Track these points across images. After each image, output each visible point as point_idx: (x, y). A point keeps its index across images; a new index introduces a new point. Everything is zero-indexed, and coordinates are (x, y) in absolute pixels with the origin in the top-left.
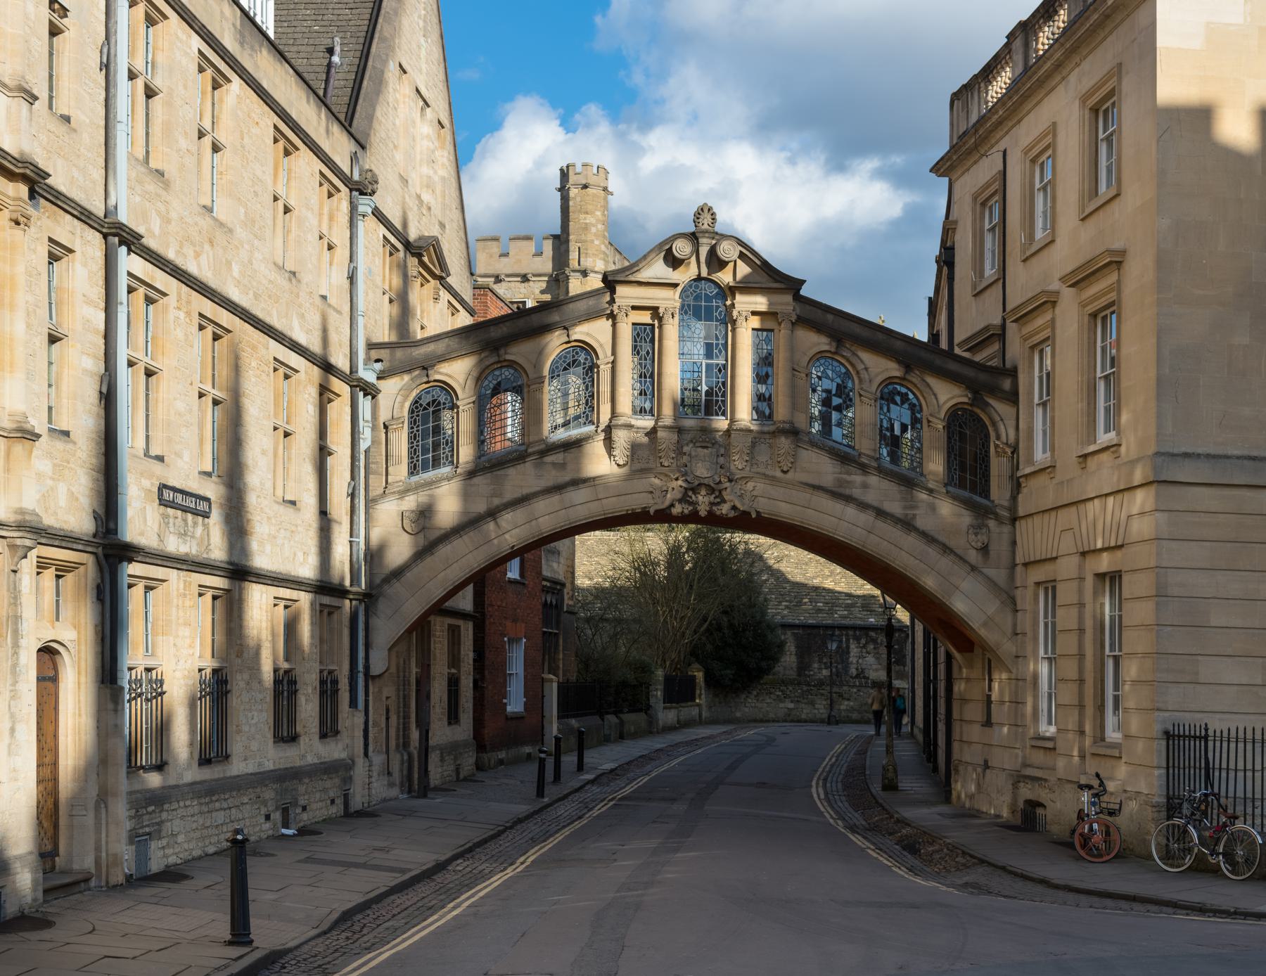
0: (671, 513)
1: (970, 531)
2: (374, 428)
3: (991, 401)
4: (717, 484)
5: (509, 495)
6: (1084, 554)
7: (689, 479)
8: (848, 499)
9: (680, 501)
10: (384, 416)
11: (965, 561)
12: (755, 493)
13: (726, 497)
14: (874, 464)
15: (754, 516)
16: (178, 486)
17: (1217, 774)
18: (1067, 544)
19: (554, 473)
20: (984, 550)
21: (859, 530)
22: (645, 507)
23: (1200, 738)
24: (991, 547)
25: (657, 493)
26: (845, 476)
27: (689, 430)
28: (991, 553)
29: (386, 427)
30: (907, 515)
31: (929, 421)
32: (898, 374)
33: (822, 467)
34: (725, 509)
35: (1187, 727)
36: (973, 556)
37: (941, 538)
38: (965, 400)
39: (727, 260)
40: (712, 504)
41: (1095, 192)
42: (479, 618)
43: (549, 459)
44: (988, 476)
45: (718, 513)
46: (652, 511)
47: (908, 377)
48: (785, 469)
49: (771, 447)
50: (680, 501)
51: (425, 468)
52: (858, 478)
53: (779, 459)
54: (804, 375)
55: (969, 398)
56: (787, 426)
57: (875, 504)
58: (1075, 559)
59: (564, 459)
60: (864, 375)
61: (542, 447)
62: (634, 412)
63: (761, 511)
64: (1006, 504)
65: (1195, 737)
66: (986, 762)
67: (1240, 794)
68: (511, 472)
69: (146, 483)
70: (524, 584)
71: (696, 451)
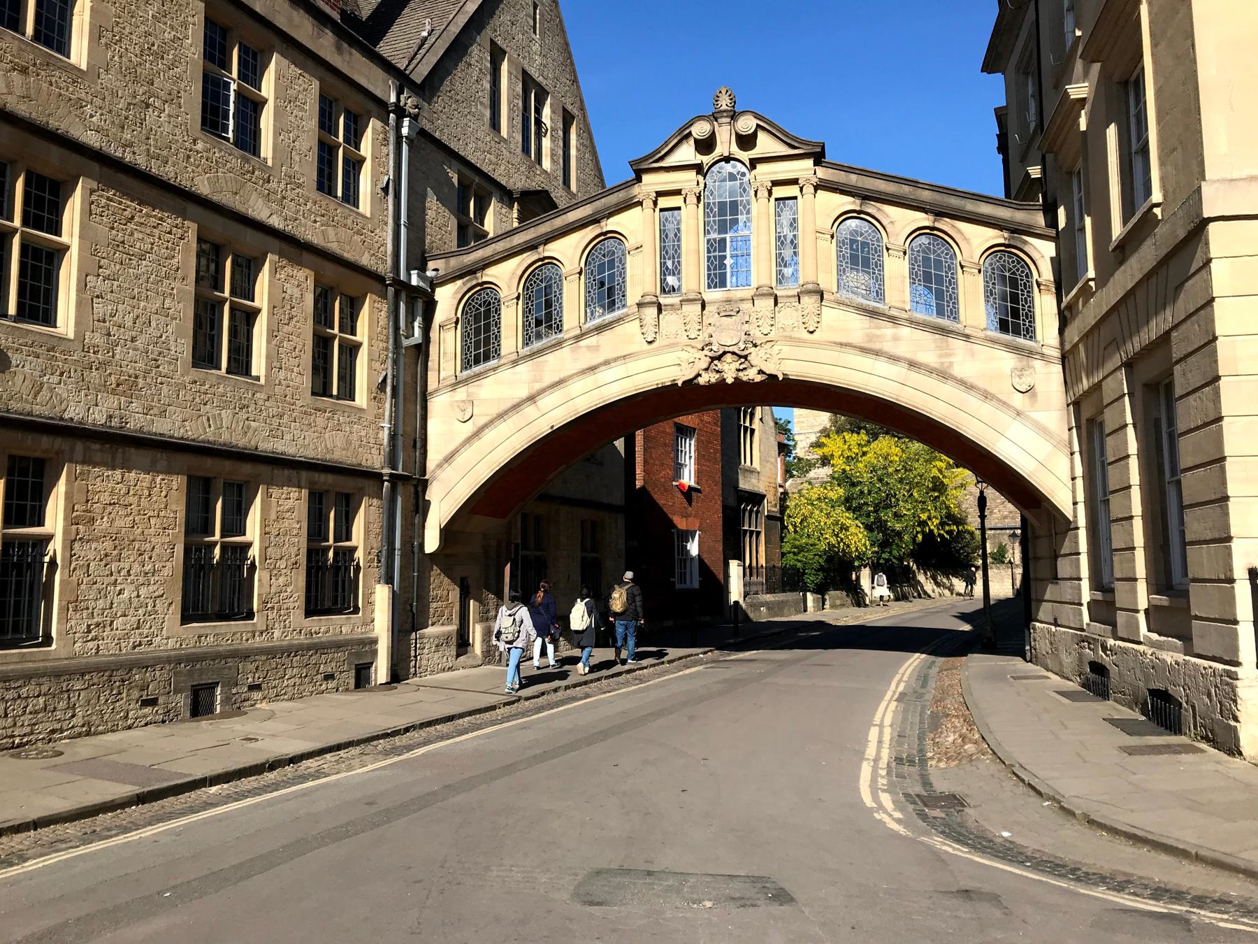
0: (698, 384)
1: (1013, 374)
4: (743, 350)
5: (548, 380)
7: (715, 348)
8: (877, 353)
9: (706, 369)
12: (779, 356)
13: (753, 363)
15: (781, 379)
22: (674, 380)
24: (1038, 389)
25: (685, 365)
26: (875, 331)
28: (1040, 396)
30: (942, 363)
31: (962, 267)
32: (927, 224)
34: (751, 375)
37: (980, 384)
39: (744, 134)
40: (738, 370)
43: (583, 343)
44: (1033, 317)
45: (745, 379)
46: (680, 385)
47: (937, 225)
48: (811, 330)
51: (477, 362)
52: (887, 330)
53: (804, 321)
54: (829, 237)
55: (1005, 239)
56: (810, 287)
57: (909, 356)
59: (598, 342)
61: (578, 332)
62: (663, 291)
63: (788, 373)
66: (1055, 619)
71: (720, 321)
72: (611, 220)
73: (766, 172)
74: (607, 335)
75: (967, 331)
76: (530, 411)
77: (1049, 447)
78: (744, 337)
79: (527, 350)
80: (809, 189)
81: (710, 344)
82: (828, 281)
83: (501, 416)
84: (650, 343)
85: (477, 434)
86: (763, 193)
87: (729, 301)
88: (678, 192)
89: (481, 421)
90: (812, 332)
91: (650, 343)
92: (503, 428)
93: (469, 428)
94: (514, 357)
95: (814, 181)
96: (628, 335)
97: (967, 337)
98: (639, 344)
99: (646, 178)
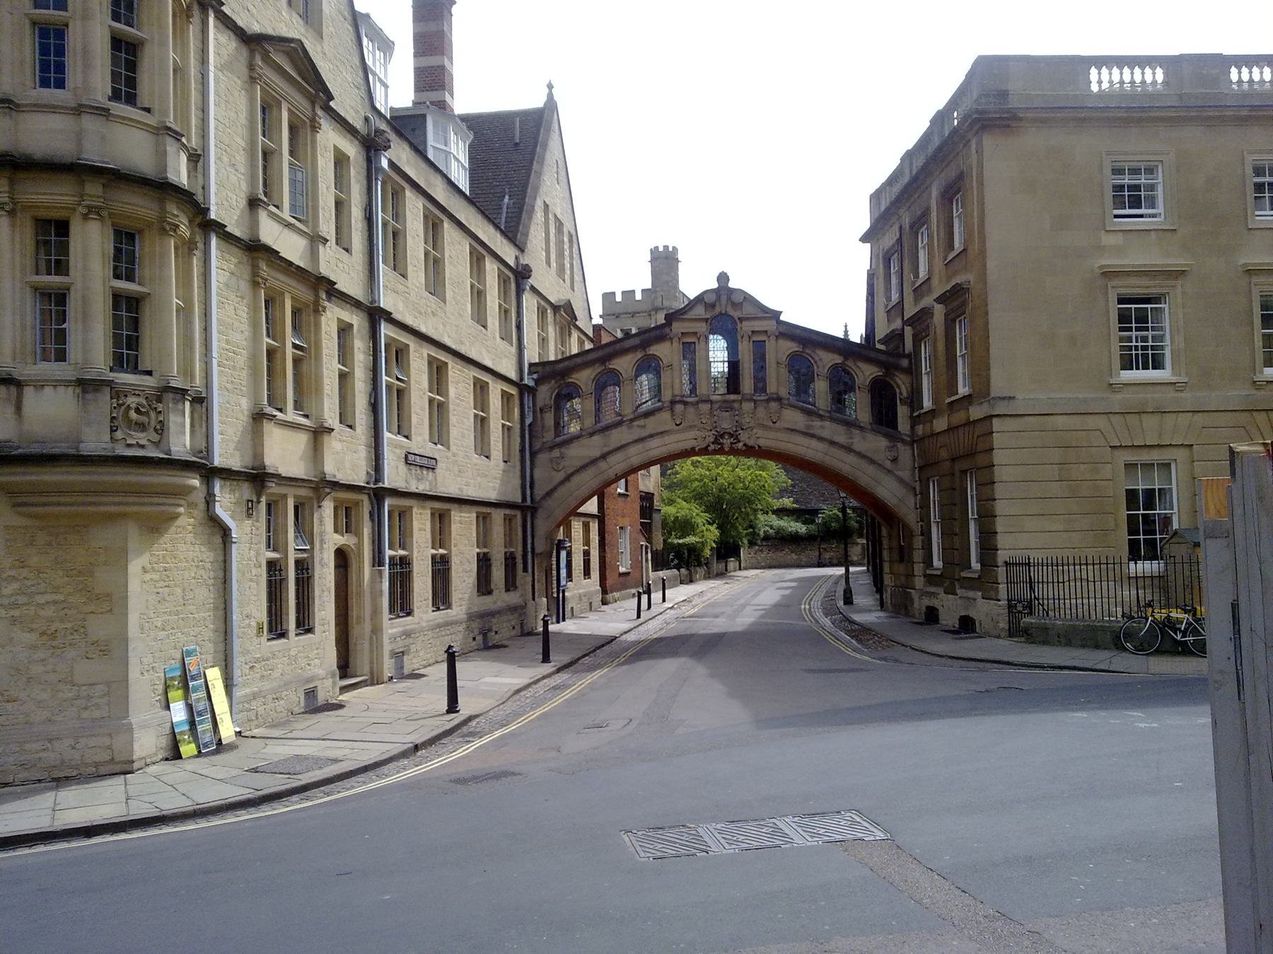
6: (953, 460)
8: (813, 436)
10: (539, 404)
11: (884, 468)
13: (742, 439)
14: (828, 415)
16: (417, 453)
17: (1036, 584)
18: (944, 454)
20: (895, 460)
21: (819, 454)
23: (1026, 564)
25: (699, 439)
27: (717, 402)
29: (541, 410)
31: (859, 388)
32: (840, 362)
34: (740, 445)
36: (888, 464)
37: (869, 455)
38: (881, 374)
40: (731, 443)
41: (951, 246)
42: (601, 517)
43: (636, 423)
46: (697, 449)
50: (713, 443)
52: (817, 423)
56: (775, 396)
57: (829, 437)
58: (948, 463)
60: (819, 363)
61: (632, 416)
64: (908, 433)
65: (1022, 564)
68: (613, 431)
69: (398, 451)
70: (628, 495)
72: (652, 348)
74: (652, 418)
75: (862, 425)
76: (603, 465)
78: (735, 423)
80: (773, 338)
81: (716, 427)
82: (783, 392)
83: (584, 467)
84: (677, 425)
86: (746, 338)
87: (725, 401)
88: (695, 333)
89: (571, 470)
91: (677, 425)
93: (560, 476)
94: (591, 431)
97: (861, 428)
98: (670, 426)
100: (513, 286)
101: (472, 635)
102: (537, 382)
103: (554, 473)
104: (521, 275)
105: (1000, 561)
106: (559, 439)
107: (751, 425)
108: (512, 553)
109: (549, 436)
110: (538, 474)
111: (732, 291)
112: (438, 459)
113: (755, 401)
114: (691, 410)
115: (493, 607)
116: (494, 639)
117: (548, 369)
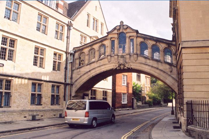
2: (74, 60)
3: (172, 46)
8: (147, 65)
9: (118, 67)
15: (131, 68)
19: (99, 64)
20: (171, 72)
24: (173, 71)
29: (76, 59)
33: (142, 60)
34: (126, 68)
35: (199, 102)
36: (169, 73)
37: (164, 70)
40: (123, 67)
46: (114, 69)
49: (134, 57)
50: (118, 67)
52: (148, 61)
56: (135, 53)
57: (152, 65)
61: (97, 60)
64: (175, 64)
67: (203, 117)
73: (128, 35)
75: (161, 61)
76: (89, 73)
77: (174, 81)
79: (89, 63)
80: (135, 38)
83: (85, 74)
84: (109, 62)
85: (81, 77)
86: (128, 38)
87: (122, 55)
88: (114, 37)
89: (82, 75)
90: (136, 61)
92: (85, 76)
94: (87, 64)
95: (136, 36)
96: (106, 60)
97: (161, 62)
98: (107, 63)
99: (109, 35)
100: (66, 28)
101: (23, 116)
102: (75, 52)
103: (78, 75)
104: (69, 26)
105: (185, 102)
106: (80, 67)
107: (129, 62)
108: (57, 96)
109: (77, 66)
110: (74, 76)
111: (123, 25)
112: (4, 64)
113: (130, 55)
114: (113, 58)
115: (41, 109)
116: (37, 117)
117: (78, 49)
